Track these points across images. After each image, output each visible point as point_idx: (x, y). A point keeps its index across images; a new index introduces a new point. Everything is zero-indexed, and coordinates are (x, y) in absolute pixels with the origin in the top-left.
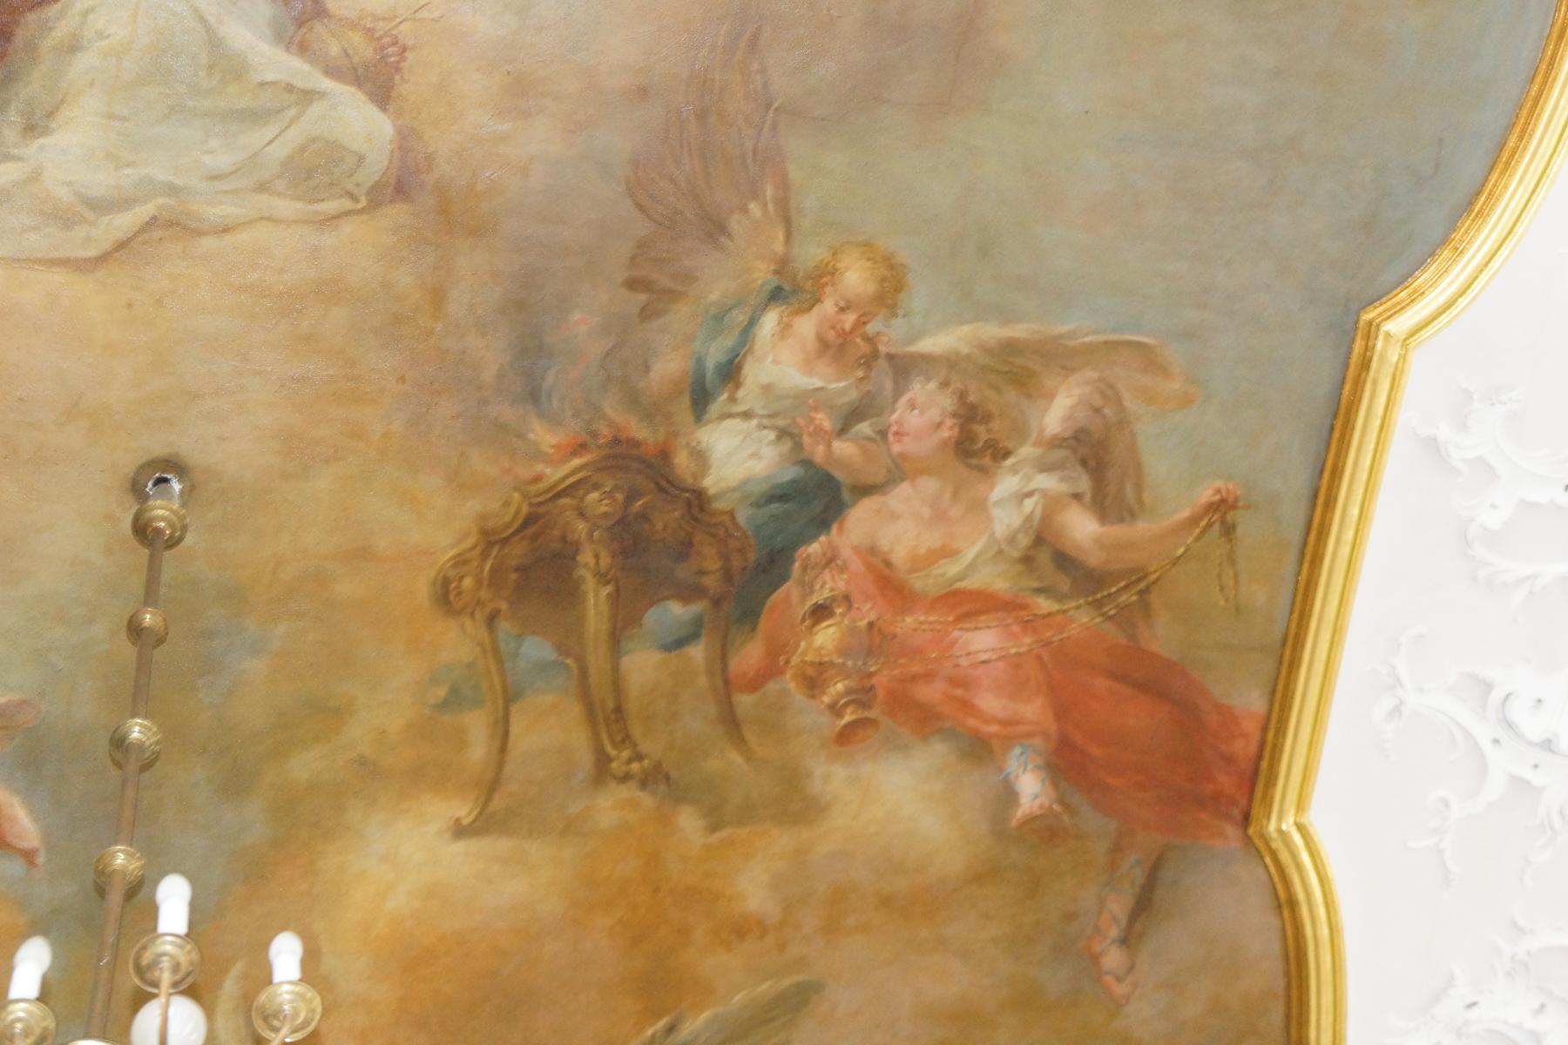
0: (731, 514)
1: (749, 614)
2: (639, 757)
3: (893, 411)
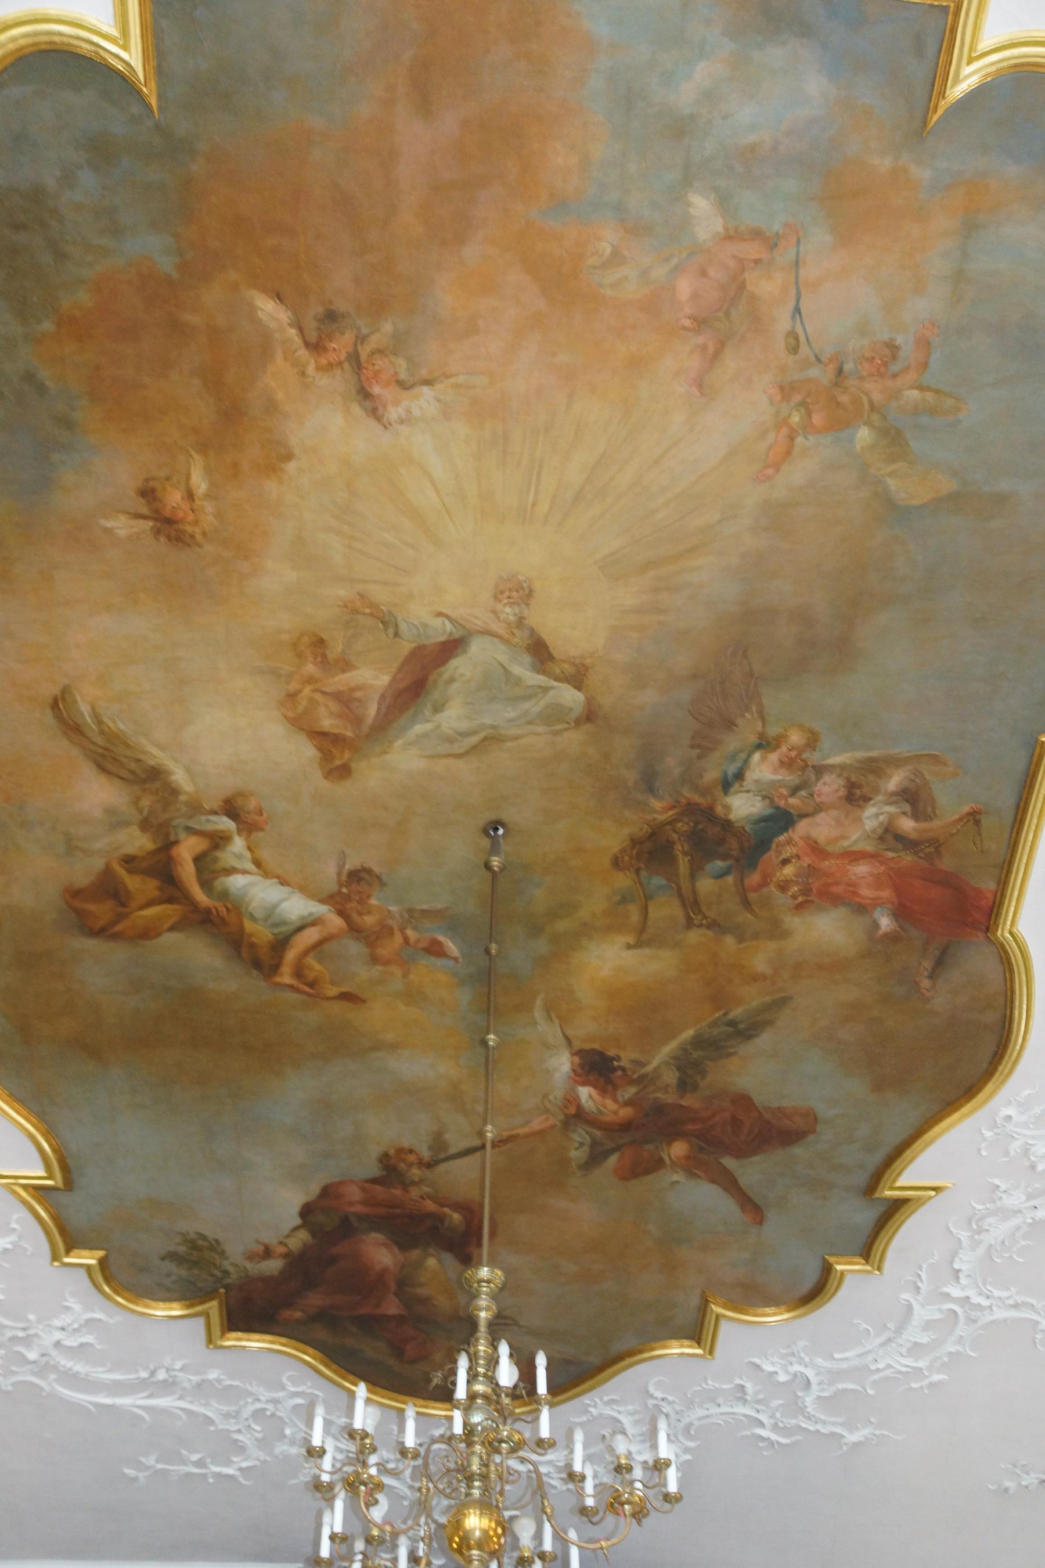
0: (743, 828)
1: (753, 864)
2: (706, 918)
3: (816, 786)
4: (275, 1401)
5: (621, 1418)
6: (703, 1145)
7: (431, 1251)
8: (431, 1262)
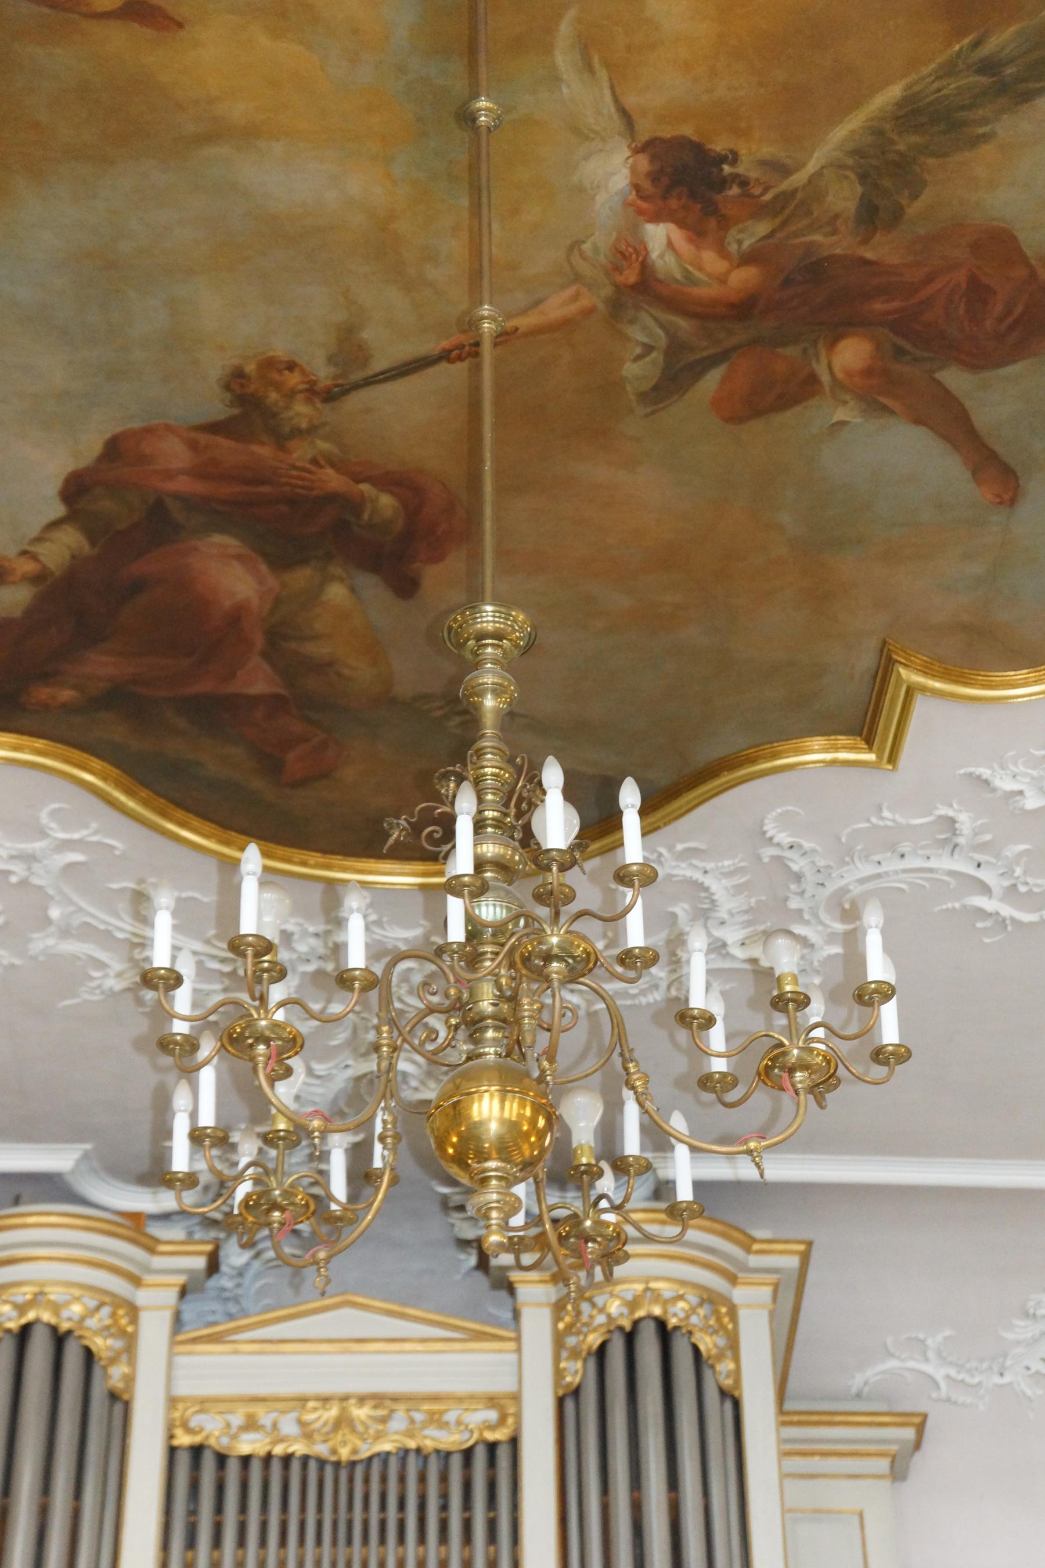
4: (29, 858)
5: (708, 881)
6: (908, 346)
7: (336, 569)
8: (336, 592)
